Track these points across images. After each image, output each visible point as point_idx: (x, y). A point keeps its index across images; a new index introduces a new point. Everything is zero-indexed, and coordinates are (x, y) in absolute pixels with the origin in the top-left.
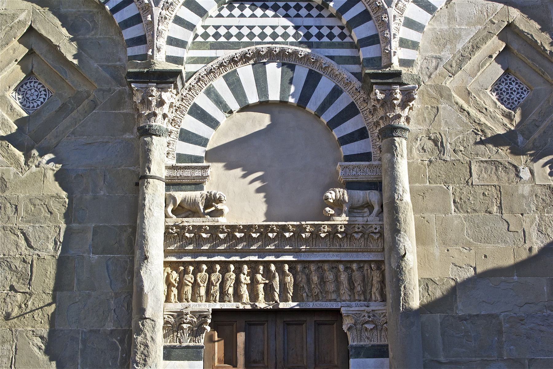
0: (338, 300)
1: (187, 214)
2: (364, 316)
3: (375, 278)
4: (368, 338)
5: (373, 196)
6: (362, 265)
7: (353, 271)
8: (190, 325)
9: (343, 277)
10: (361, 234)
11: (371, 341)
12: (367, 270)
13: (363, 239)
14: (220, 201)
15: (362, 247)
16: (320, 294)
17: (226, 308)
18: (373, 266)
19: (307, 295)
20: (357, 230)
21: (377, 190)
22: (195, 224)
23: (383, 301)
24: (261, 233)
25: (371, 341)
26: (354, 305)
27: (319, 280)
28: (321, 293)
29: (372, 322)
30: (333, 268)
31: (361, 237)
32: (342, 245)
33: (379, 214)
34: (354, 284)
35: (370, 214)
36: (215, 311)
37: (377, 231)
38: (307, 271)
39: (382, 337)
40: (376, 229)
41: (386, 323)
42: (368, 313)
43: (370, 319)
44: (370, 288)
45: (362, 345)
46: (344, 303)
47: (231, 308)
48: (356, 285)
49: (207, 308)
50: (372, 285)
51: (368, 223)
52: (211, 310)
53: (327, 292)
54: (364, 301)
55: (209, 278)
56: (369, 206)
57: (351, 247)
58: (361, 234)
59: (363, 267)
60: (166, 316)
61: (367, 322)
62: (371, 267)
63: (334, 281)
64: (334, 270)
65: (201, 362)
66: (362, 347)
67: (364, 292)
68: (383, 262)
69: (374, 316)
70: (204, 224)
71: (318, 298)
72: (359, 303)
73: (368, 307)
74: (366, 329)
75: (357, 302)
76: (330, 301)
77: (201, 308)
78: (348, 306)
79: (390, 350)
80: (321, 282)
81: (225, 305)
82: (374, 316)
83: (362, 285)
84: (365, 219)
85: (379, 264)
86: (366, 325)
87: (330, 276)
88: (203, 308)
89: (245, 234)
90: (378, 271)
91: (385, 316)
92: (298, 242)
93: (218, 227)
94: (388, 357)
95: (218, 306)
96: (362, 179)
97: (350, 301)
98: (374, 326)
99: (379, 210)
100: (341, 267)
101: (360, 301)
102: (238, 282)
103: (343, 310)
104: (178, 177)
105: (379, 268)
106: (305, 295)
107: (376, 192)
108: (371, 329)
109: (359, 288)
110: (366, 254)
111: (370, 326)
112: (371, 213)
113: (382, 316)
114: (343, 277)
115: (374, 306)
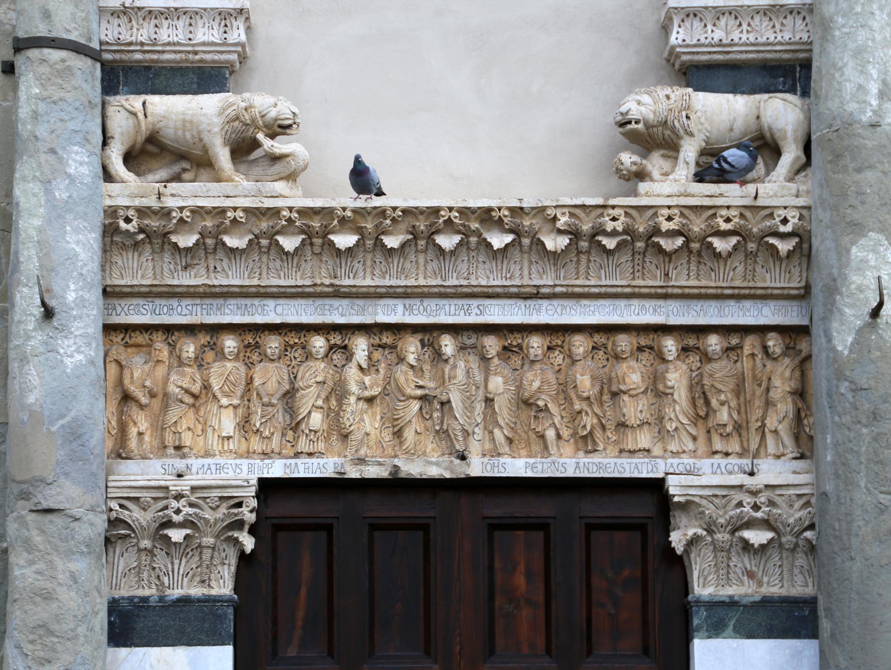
0: (657, 451)
1: (176, 168)
2: (740, 504)
3: (777, 382)
4: (751, 575)
5: (781, 111)
6: (734, 341)
7: (706, 358)
8: (188, 531)
9: (677, 378)
10: (734, 240)
11: (760, 584)
12: (753, 355)
13: (741, 256)
14: (280, 129)
15: (737, 283)
16: (598, 434)
17: (302, 475)
18: (770, 343)
19: (559, 437)
20: (724, 226)
21: (792, 90)
22: (201, 203)
23: (802, 457)
24: (414, 233)
25: (760, 584)
26: (709, 471)
27: (597, 389)
28: (603, 428)
29: (766, 524)
30: (640, 349)
31: (735, 248)
32: (673, 274)
33: (798, 172)
34: (707, 402)
35: (768, 173)
36: (268, 488)
37: (788, 228)
38: (558, 358)
39: (796, 571)
40: (785, 221)
41: (811, 527)
42: (754, 493)
43: (759, 515)
44: (759, 413)
45: (731, 597)
46: (675, 461)
47: (318, 475)
48: (714, 403)
49: (244, 475)
50: (769, 404)
51: (760, 202)
52: (254, 482)
53: (622, 425)
54: (740, 455)
55: (250, 381)
56: (764, 146)
57: (703, 283)
58: (734, 240)
59: (740, 347)
60: (114, 505)
61: (750, 524)
62: (765, 348)
63: (645, 392)
64: (645, 356)
65: (228, 651)
66: (732, 604)
67: (738, 428)
68: (803, 331)
69: (771, 503)
70: (228, 203)
71: (595, 443)
72: (723, 462)
73: (752, 474)
74: (746, 546)
75: (718, 460)
76: (632, 452)
77: (223, 476)
78: (689, 473)
79: (821, 613)
80: (601, 393)
81: (301, 468)
82: (771, 503)
83: (733, 404)
84: (751, 188)
85: (794, 334)
86: (747, 534)
87: (633, 375)
88: (231, 474)
89: (363, 238)
90: (787, 361)
91: (808, 504)
92: (531, 263)
93: (275, 212)
94: (813, 634)
95: (277, 469)
96: (744, 56)
97: (694, 453)
98: (770, 535)
99: (797, 158)
100: (670, 345)
101: (727, 454)
102: (338, 392)
103: (675, 487)
104: (142, 44)
105: (789, 350)
106: (551, 434)
107: (788, 96)
108: (763, 547)
109: (723, 416)
110: (747, 304)
111: (757, 537)
112: (770, 169)
113: (797, 505)
114: (677, 378)
115: (775, 471)
